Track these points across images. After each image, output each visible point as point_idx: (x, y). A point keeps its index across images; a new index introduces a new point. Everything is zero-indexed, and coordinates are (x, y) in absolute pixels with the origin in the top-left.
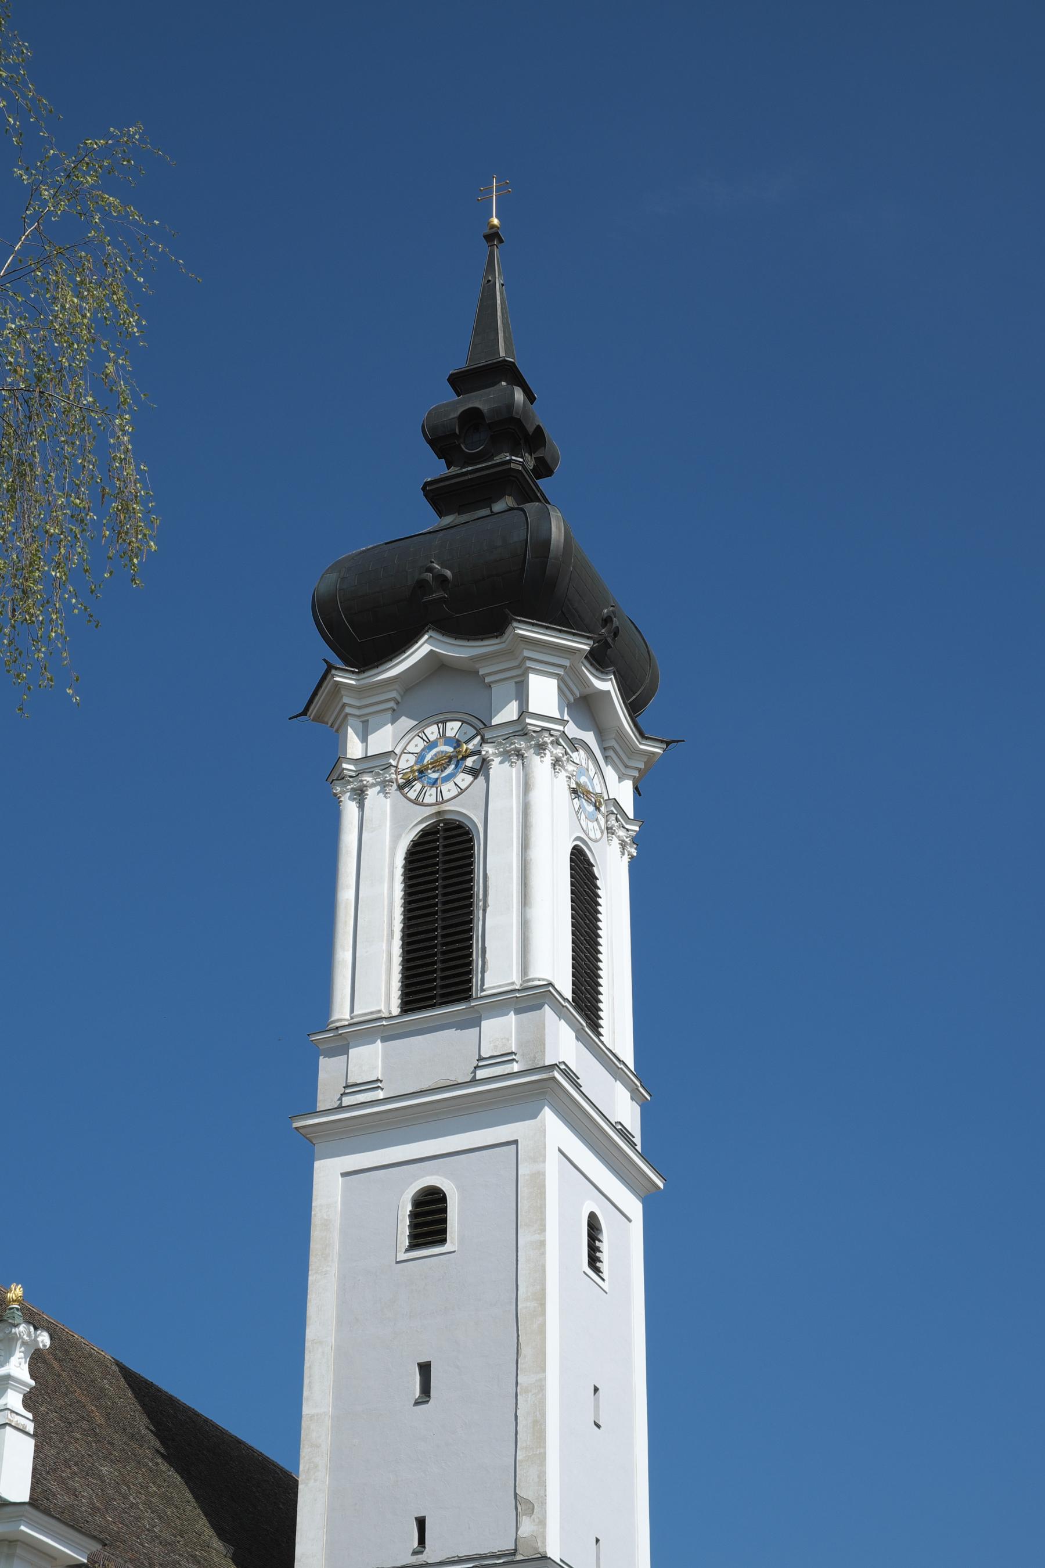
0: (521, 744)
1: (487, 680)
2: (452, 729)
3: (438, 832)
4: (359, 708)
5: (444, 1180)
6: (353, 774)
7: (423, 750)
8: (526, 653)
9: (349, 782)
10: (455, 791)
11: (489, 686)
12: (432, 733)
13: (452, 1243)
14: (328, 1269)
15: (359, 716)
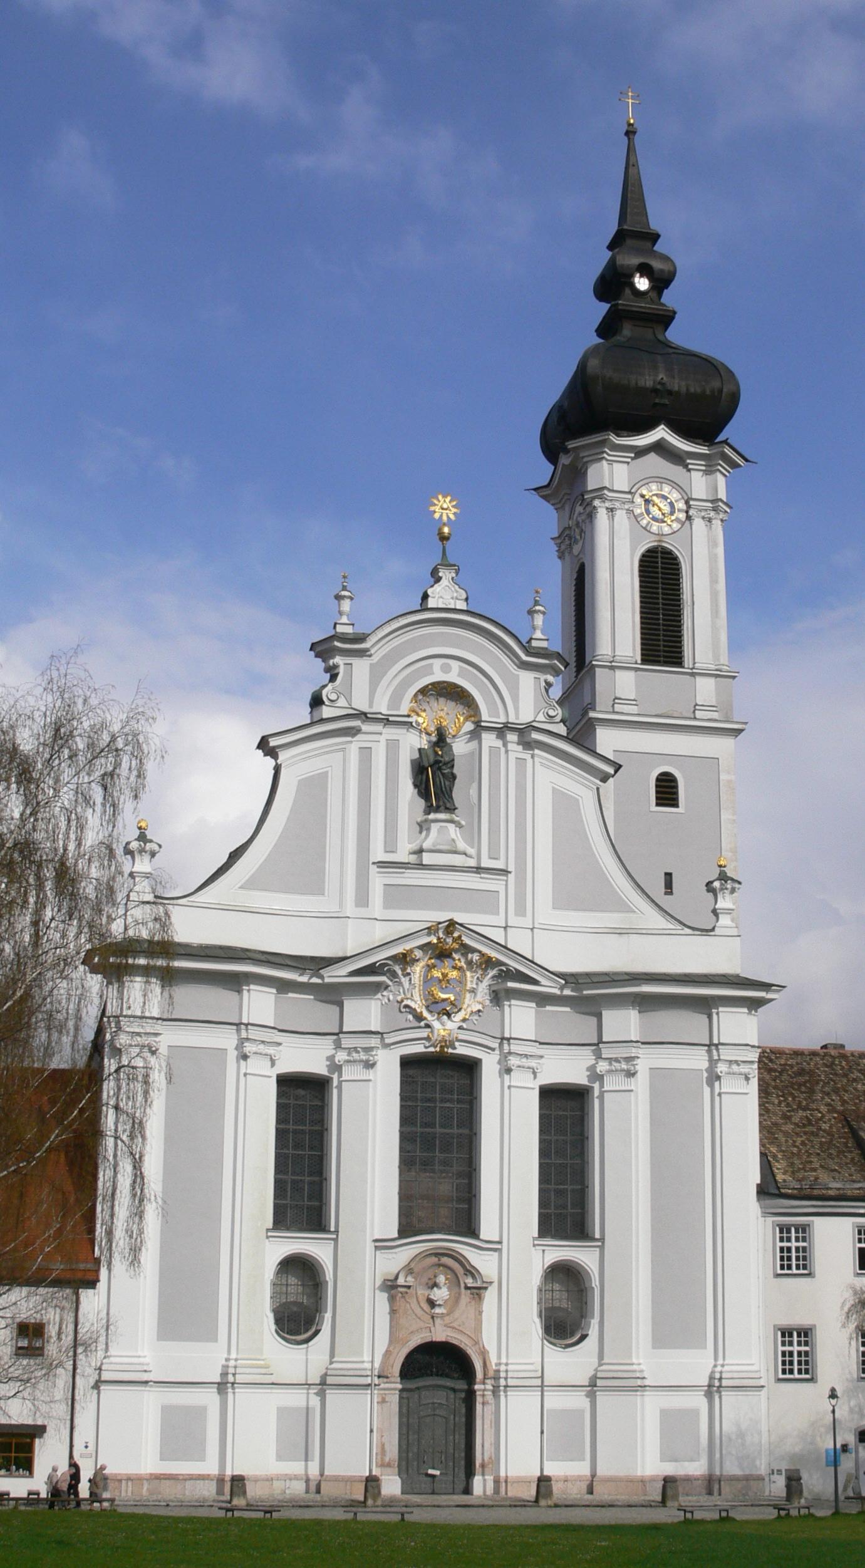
0: (712, 514)
1: (690, 467)
9: (604, 502)
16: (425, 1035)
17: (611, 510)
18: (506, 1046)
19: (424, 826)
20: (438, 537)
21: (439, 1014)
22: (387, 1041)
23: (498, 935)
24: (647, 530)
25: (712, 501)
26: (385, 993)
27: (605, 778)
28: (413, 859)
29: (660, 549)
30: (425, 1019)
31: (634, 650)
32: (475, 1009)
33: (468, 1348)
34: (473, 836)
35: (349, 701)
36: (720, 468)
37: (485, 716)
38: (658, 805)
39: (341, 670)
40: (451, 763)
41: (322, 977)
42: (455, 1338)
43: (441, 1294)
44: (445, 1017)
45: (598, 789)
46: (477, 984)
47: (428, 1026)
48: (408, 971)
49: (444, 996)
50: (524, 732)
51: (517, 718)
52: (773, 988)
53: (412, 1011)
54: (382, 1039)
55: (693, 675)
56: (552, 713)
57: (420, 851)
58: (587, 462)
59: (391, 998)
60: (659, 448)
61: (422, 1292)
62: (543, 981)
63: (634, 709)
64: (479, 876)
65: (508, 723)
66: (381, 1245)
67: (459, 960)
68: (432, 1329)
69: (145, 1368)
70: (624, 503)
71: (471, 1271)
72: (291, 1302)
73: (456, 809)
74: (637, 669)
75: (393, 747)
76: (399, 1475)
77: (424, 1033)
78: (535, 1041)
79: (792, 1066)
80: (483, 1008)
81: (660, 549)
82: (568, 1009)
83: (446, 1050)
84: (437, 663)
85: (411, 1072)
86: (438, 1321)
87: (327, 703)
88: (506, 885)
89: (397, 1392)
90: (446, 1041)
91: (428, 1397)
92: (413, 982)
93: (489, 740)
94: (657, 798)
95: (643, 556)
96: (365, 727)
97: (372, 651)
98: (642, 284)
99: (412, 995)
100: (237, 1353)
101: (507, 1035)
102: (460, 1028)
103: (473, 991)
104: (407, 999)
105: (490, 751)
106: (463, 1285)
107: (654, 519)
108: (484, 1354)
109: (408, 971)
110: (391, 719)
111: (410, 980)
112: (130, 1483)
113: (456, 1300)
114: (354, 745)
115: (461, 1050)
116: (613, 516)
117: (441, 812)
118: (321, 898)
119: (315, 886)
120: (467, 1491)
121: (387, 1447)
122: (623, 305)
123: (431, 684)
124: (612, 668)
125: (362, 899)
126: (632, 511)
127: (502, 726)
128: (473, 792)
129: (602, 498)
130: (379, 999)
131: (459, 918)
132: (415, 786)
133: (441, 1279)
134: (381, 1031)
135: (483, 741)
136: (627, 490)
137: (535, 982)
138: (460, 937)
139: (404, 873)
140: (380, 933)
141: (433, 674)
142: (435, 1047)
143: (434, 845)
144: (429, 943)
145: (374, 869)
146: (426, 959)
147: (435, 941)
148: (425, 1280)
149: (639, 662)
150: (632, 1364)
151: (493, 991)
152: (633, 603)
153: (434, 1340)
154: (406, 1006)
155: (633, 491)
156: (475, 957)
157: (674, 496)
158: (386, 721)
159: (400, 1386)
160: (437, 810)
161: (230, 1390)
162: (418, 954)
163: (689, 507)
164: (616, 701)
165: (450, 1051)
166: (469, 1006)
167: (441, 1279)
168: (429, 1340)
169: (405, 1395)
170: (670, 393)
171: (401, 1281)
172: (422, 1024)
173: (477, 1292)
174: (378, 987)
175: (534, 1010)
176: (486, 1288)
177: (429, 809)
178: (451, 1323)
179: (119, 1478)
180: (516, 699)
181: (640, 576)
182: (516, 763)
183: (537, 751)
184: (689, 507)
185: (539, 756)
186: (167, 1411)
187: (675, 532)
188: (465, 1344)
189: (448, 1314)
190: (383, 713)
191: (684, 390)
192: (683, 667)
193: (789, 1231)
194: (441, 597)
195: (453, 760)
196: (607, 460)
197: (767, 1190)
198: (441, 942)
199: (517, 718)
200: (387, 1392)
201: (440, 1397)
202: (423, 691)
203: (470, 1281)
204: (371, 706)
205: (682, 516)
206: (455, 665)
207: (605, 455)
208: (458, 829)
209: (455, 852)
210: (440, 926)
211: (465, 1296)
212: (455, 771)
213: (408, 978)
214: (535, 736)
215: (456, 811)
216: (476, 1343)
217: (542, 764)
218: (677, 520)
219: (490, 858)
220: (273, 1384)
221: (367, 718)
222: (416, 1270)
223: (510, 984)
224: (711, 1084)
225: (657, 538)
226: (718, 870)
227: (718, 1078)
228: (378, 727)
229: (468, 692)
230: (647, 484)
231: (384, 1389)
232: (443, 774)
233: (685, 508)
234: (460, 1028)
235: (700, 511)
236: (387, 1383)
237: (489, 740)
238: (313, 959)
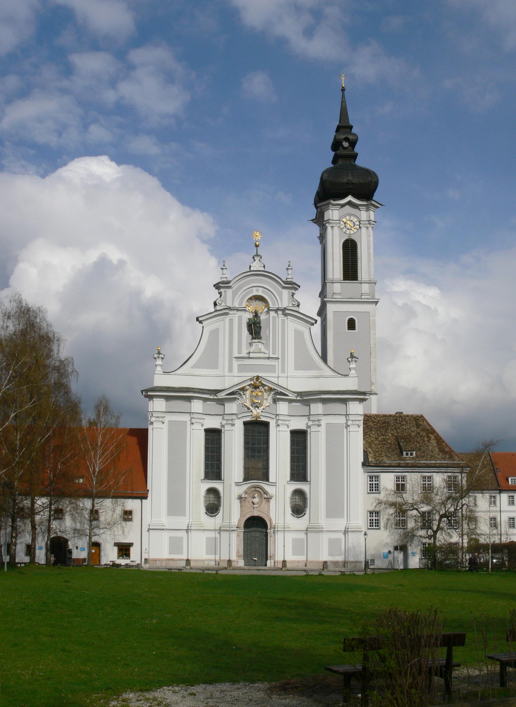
0: (368, 225)
1: (361, 209)
3: (349, 240)
8: (371, 207)
16: (250, 414)
17: (332, 227)
18: (277, 417)
19: (251, 344)
20: (255, 246)
21: (255, 407)
22: (238, 417)
23: (275, 380)
25: (368, 221)
26: (238, 401)
28: (247, 356)
30: (250, 409)
31: (340, 276)
34: (267, 348)
36: (371, 209)
37: (271, 306)
38: (348, 329)
39: (223, 294)
41: (217, 396)
43: (256, 500)
44: (257, 408)
46: (268, 397)
47: (251, 411)
48: (245, 393)
49: (257, 401)
51: (282, 305)
53: (246, 407)
54: (237, 416)
55: (361, 283)
56: (294, 303)
57: (249, 353)
58: (324, 211)
59: (240, 402)
60: (350, 203)
61: (250, 500)
65: (279, 308)
66: (237, 484)
69: (163, 525)
71: (266, 493)
72: (211, 503)
73: (261, 338)
74: (341, 283)
75: (240, 318)
76: (244, 560)
77: (250, 414)
79: (382, 420)
82: (299, 404)
84: (255, 289)
85: (247, 427)
86: (255, 509)
87: (218, 304)
88: (278, 363)
89: (243, 532)
91: (253, 534)
93: (272, 314)
94: (348, 327)
95: (344, 242)
96: (230, 312)
97: (233, 286)
98: (346, 144)
101: (278, 413)
102: (262, 412)
103: (266, 399)
106: (263, 497)
107: (348, 229)
108: (270, 520)
109: (245, 393)
110: (239, 309)
111: (246, 396)
113: (262, 501)
114: (227, 318)
115: (263, 419)
116: (333, 229)
119: (215, 366)
120: (266, 565)
121: (240, 551)
122: (338, 153)
123: (253, 296)
124: (332, 283)
125: (231, 370)
128: (267, 332)
129: (328, 223)
130: (236, 403)
131: (260, 375)
132: (248, 331)
133: (256, 495)
134: (236, 413)
135: (270, 314)
136: (338, 219)
138: (261, 381)
140: (237, 381)
141: (253, 292)
142: (254, 418)
143: (254, 350)
144: (251, 384)
145: (234, 360)
146: (251, 389)
147: (253, 383)
148: (251, 496)
149: (342, 280)
151: (274, 399)
154: (244, 405)
156: (266, 388)
157: (355, 220)
158: (238, 310)
159: (243, 531)
160: (255, 339)
162: (248, 387)
163: (360, 223)
165: (259, 419)
167: (256, 495)
168: (252, 515)
169: (246, 533)
170: (353, 184)
171: (243, 496)
172: (250, 411)
173: (268, 499)
174: (235, 399)
175: (287, 405)
176: (271, 498)
177: (253, 338)
181: (343, 250)
182: (282, 321)
183: (289, 317)
184: (360, 223)
185: (289, 318)
186: (171, 539)
189: (258, 507)
190: (237, 307)
191: (358, 182)
192: (358, 281)
193: (372, 478)
194: (255, 267)
195: (260, 321)
196: (331, 209)
197: (365, 464)
201: (257, 534)
202: (250, 299)
203: (265, 496)
204: (233, 305)
205: (358, 227)
206: (261, 289)
207: (330, 208)
208: (262, 345)
209: (261, 353)
210: (254, 378)
212: (261, 325)
213: (245, 395)
214: (287, 312)
216: (268, 516)
219: (273, 354)
222: (248, 492)
223: (278, 397)
224: (346, 428)
225: (349, 235)
227: (349, 426)
228: (235, 312)
231: (239, 532)
233: (359, 224)
234: (262, 412)
235: (364, 224)
237: (272, 314)
238: (215, 390)
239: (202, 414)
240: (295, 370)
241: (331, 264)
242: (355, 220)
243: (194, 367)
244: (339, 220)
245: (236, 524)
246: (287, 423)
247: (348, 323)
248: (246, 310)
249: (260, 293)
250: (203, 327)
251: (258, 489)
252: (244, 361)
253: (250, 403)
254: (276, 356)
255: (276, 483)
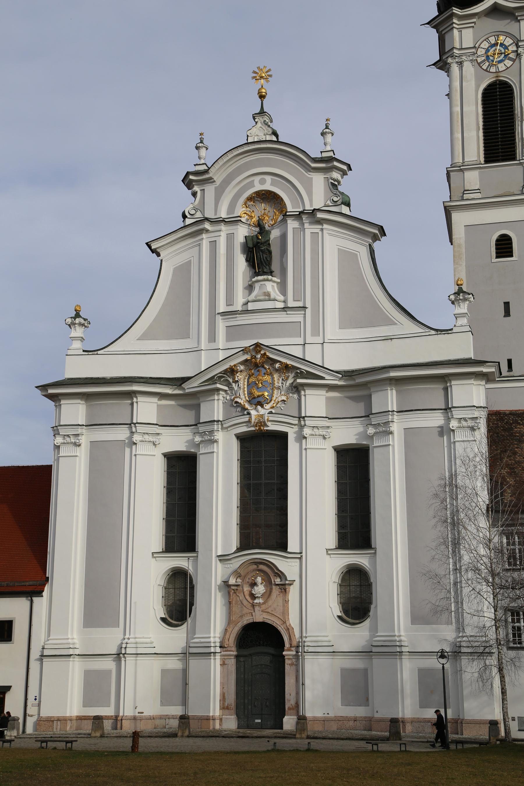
1: (519, 18)
2: (508, 42)
4: (458, 25)
5: (510, 232)
6: (458, 55)
7: (488, 47)
9: (455, 58)
10: (504, 68)
11: (519, 21)
12: (492, 40)
13: (515, 257)
14: (462, 263)
15: (457, 29)
17: (460, 64)
18: (302, 423)
20: (257, 96)
22: (224, 426)
23: (297, 352)
24: (487, 71)
27: (375, 238)
29: (498, 82)
30: (247, 409)
32: (279, 401)
33: (278, 626)
34: (283, 288)
35: (203, 213)
37: (290, 208)
40: (268, 243)
41: (184, 389)
42: (269, 619)
44: (259, 407)
45: (370, 245)
49: (260, 394)
50: (314, 215)
51: (311, 205)
52: (487, 364)
56: (335, 199)
57: (246, 304)
62: (327, 377)
63: (479, 195)
64: (286, 313)
66: (223, 558)
67: (269, 368)
68: (253, 613)
70: (469, 56)
71: (280, 574)
77: (246, 419)
78: (326, 417)
80: (287, 399)
81: (498, 82)
83: (262, 428)
84: (257, 179)
86: (257, 608)
87: (188, 217)
88: (305, 317)
90: (261, 422)
92: (240, 386)
95: (485, 90)
99: (240, 395)
100: (130, 635)
102: (271, 413)
103: (279, 388)
104: (237, 397)
105: (293, 230)
108: (289, 630)
110: (226, 220)
111: (238, 385)
112: (59, 723)
113: (271, 592)
115: (272, 427)
116: (462, 67)
117: (261, 275)
118: (188, 340)
124: (461, 170)
125: (212, 337)
126: (477, 60)
127: (298, 213)
129: (452, 56)
133: (259, 580)
136: (472, 46)
137: (323, 378)
138: (265, 354)
139: (236, 317)
141: (254, 186)
143: (255, 297)
144: (246, 361)
145: (219, 318)
149: (482, 160)
150: (395, 636)
152: (478, 124)
153: (255, 621)
154: (236, 402)
155: (477, 46)
156: (277, 365)
157: (509, 41)
159: (235, 653)
161: (123, 659)
163: (518, 46)
164: (465, 192)
165: (265, 428)
166: (277, 398)
167: (259, 580)
168: (251, 621)
169: (242, 659)
172: (246, 413)
173: (284, 588)
177: (257, 274)
178: (265, 609)
179: (52, 719)
180: (310, 194)
182: (311, 237)
183: (325, 226)
185: (327, 229)
187: (508, 68)
188: (276, 623)
189: (264, 603)
192: (517, 160)
195: (269, 240)
198: (253, 358)
199: (311, 205)
200: (226, 657)
202: (250, 199)
203: (278, 581)
204: (216, 214)
206: (268, 178)
211: (276, 591)
215: (273, 273)
216: (284, 622)
217: (330, 234)
218: (510, 59)
219: (294, 300)
220: (155, 654)
221: (226, 222)
223: (299, 381)
225: (495, 75)
226: (457, 287)
229: (278, 195)
230: (488, 38)
232: (262, 251)
234: (271, 413)
236: (226, 651)
239: (157, 424)
240: (340, 328)
241: (460, 136)
242: (509, 41)
243: (145, 337)
244: (474, 47)
245: (218, 640)
246: (324, 433)
247: (496, 245)
248: (240, 220)
249: (268, 186)
250: (162, 261)
251: (262, 567)
252: (238, 319)
253: (247, 398)
254: (300, 304)
255: (301, 553)
